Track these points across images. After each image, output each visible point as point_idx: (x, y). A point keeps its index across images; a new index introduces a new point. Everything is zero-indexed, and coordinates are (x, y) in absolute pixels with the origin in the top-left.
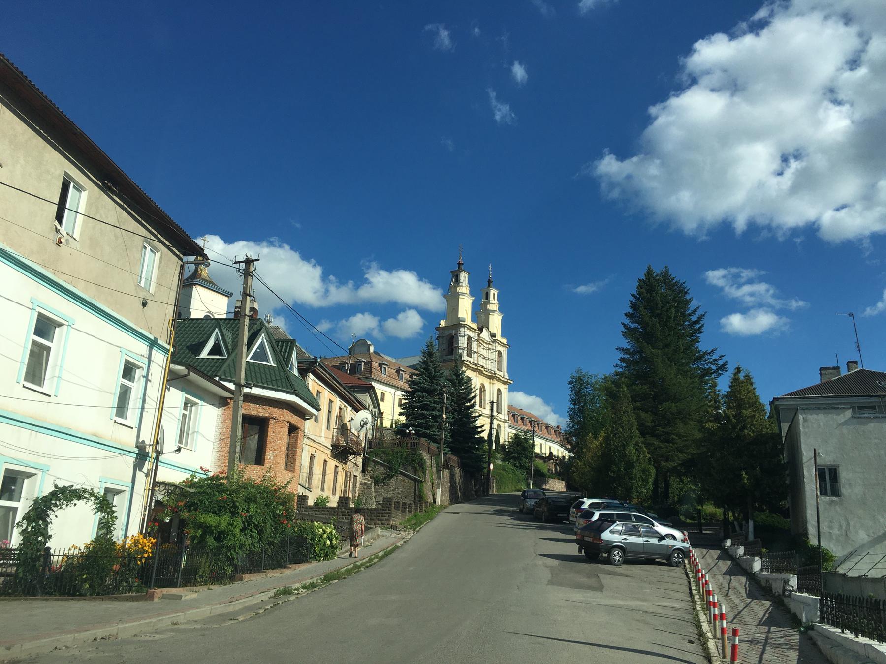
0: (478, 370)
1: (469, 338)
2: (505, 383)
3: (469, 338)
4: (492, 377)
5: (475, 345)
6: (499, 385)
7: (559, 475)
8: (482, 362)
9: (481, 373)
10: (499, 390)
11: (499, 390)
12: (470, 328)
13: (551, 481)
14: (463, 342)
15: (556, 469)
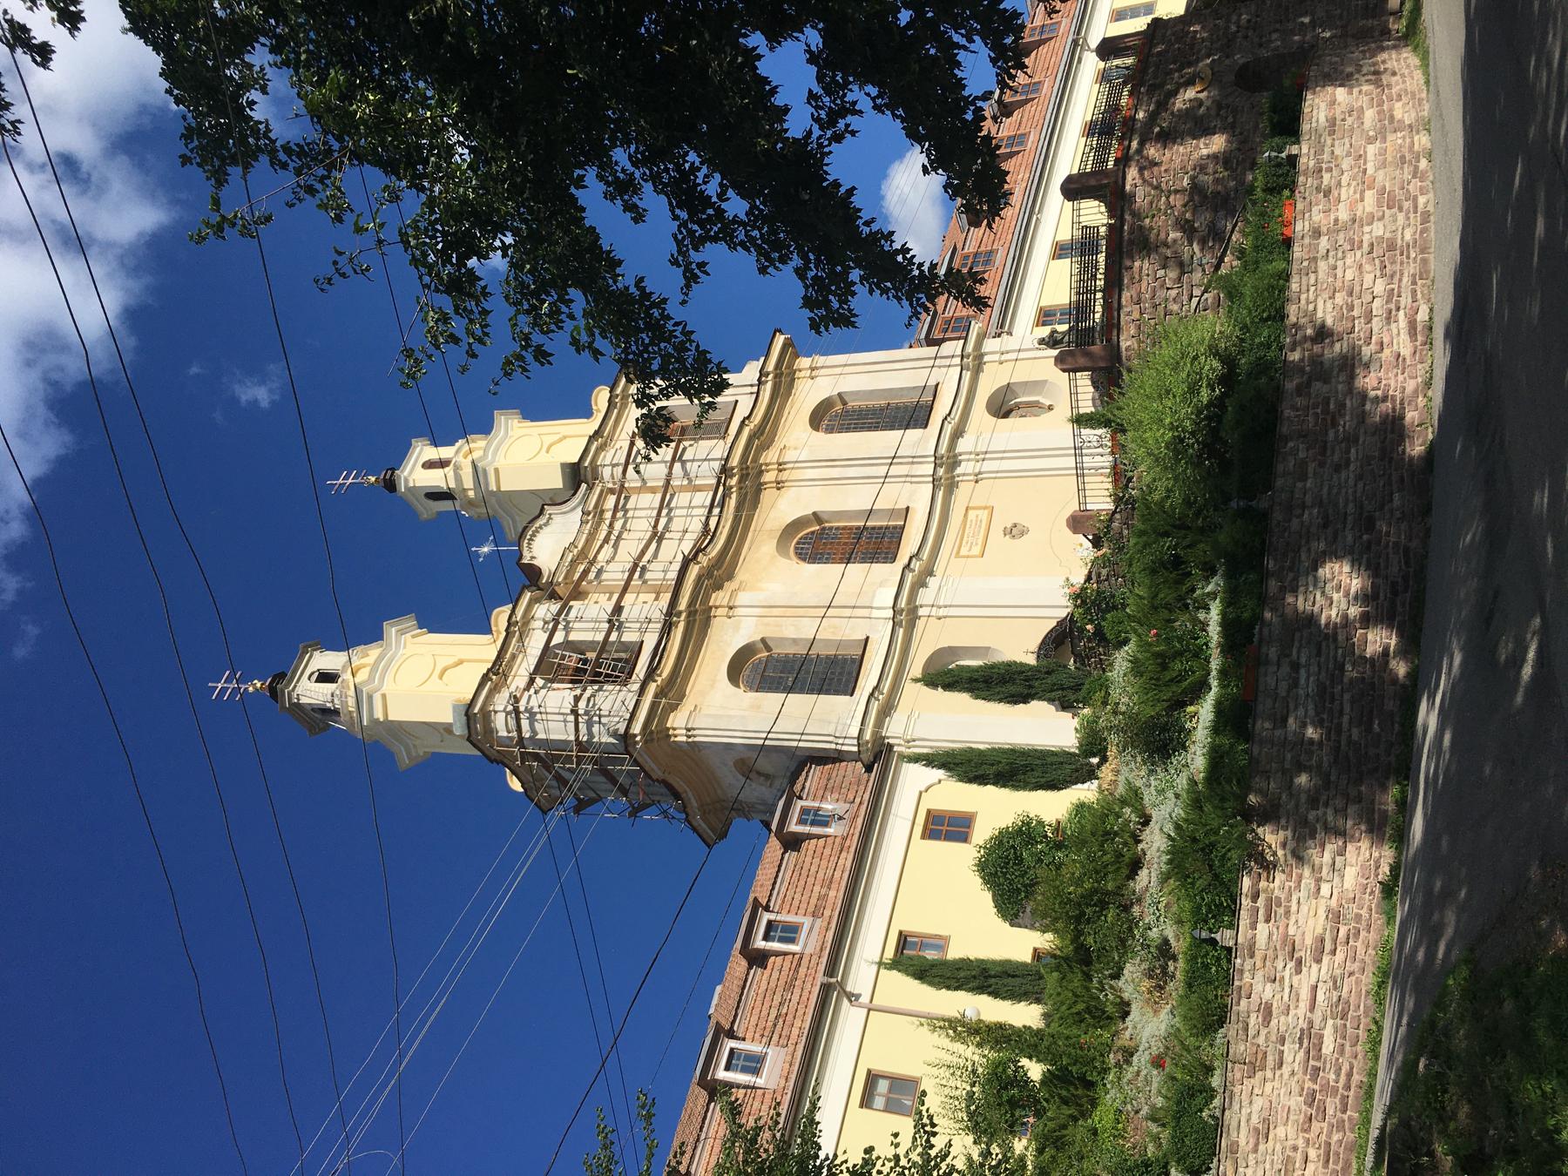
0: (691, 616)
1: (548, 668)
2: (784, 383)
3: (548, 668)
4: (745, 484)
5: (588, 621)
6: (797, 437)
7: (1251, 197)
8: (665, 566)
9: (720, 573)
10: (822, 417)
11: (822, 417)
12: (497, 672)
13: (1317, 298)
14: (554, 712)
15: (1196, 124)
